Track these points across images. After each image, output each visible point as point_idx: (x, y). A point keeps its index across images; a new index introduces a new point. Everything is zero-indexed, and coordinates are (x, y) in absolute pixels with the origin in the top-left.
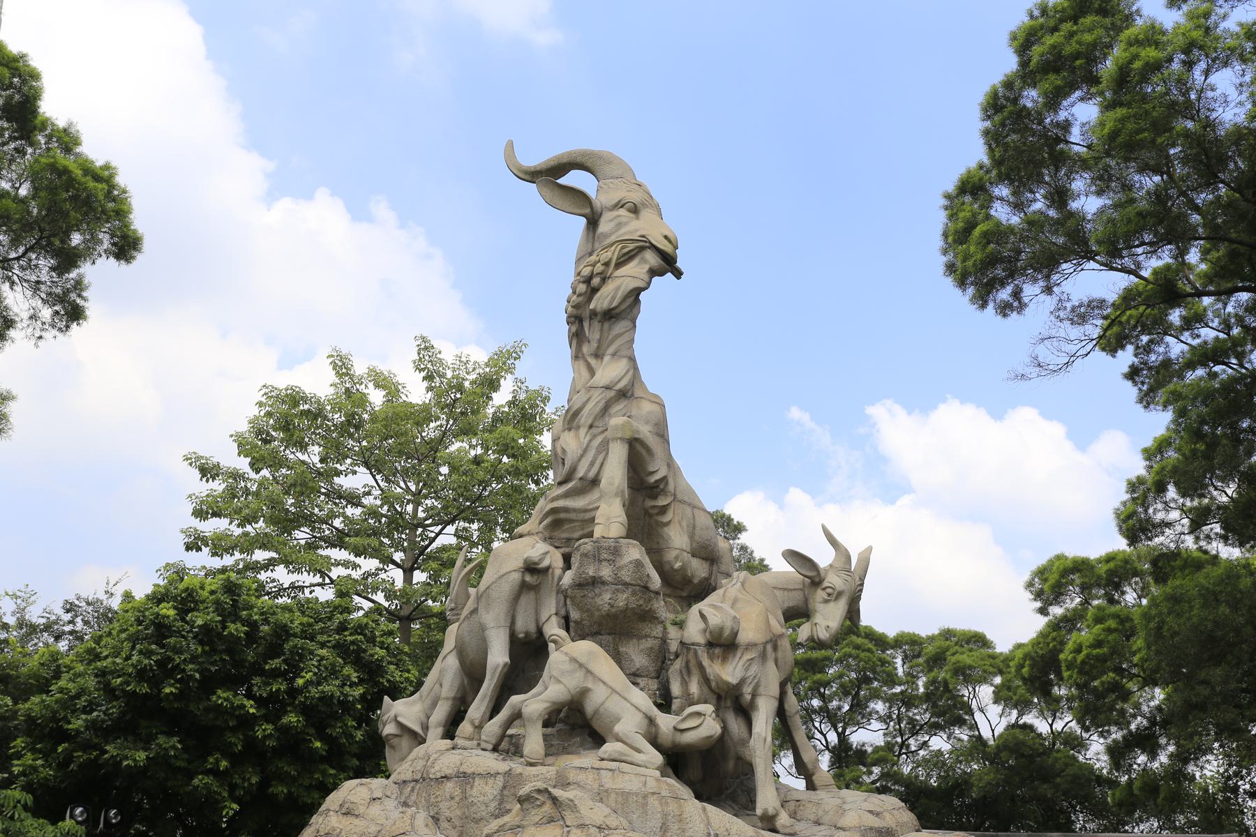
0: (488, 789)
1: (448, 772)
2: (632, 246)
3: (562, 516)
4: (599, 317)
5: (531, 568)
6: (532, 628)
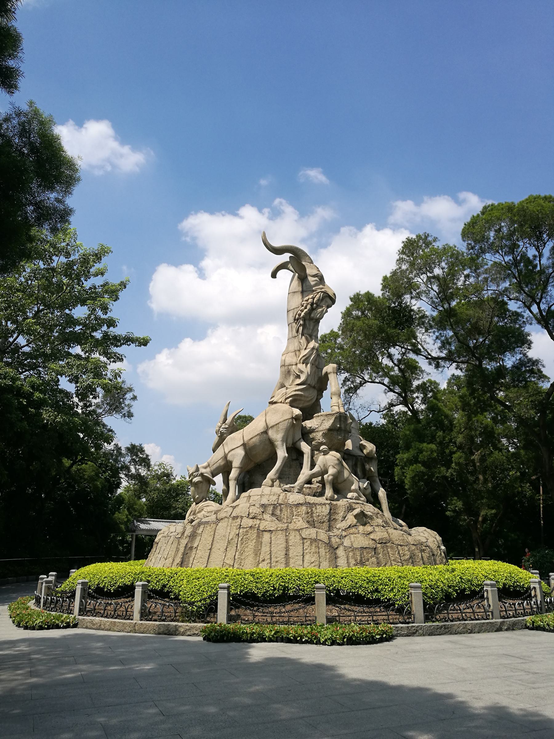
0: (324, 510)
1: (301, 502)
2: (326, 295)
3: (298, 398)
4: (314, 321)
5: (296, 418)
6: (291, 443)
